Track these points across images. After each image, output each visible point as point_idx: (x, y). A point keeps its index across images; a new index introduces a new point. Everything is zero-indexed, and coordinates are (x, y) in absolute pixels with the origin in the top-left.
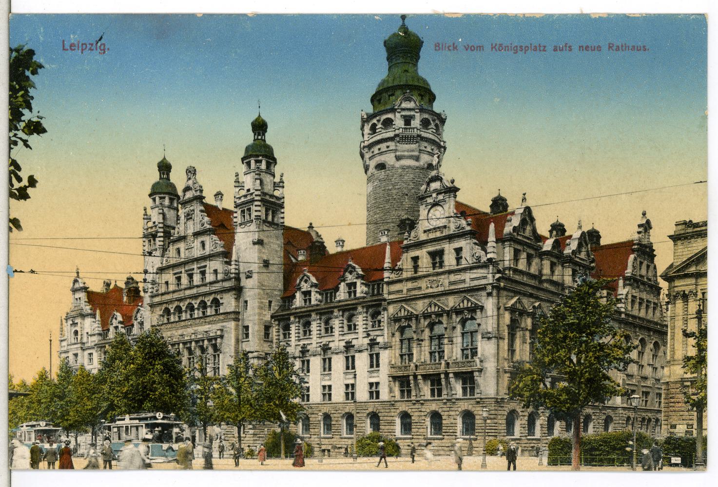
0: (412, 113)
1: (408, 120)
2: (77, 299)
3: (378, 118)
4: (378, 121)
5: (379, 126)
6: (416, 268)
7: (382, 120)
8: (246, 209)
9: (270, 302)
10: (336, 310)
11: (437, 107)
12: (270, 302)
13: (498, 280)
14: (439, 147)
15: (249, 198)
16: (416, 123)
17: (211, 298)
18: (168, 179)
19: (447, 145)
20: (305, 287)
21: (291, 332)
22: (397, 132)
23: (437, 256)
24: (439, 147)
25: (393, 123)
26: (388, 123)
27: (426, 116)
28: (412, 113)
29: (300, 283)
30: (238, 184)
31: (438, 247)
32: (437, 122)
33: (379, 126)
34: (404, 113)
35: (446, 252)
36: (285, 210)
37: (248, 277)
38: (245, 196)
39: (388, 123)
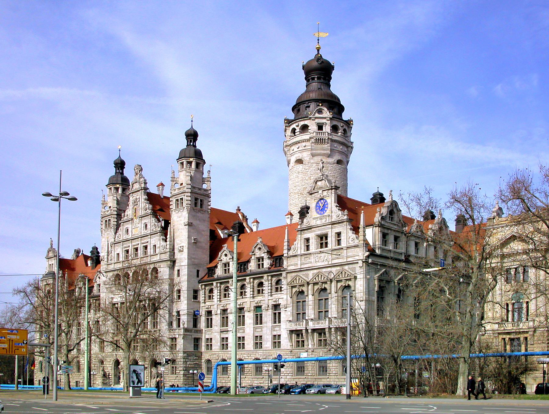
0: (324, 121)
1: (320, 127)
3: (297, 124)
4: (297, 126)
5: (298, 130)
6: (308, 247)
7: (300, 126)
8: (179, 198)
9: (198, 271)
10: (247, 278)
11: (345, 116)
12: (198, 271)
13: (368, 257)
14: (347, 147)
15: (182, 190)
16: (327, 129)
18: (122, 173)
19: (354, 145)
20: (225, 259)
21: (214, 294)
22: (312, 135)
23: (323, 239)
24: (347, 147)
25: (309, 128)
26: (305, 128)
27: (335, 123)
28: (324, 121)
29: (221, 256)
30: (174, 180)
31: (324, 232)
32: (345, 127)
33: (298, 130)
34: (317, 120)
35: (329, 236)
36: (212, 199)
38: (179, 189)
39: (305, 128)
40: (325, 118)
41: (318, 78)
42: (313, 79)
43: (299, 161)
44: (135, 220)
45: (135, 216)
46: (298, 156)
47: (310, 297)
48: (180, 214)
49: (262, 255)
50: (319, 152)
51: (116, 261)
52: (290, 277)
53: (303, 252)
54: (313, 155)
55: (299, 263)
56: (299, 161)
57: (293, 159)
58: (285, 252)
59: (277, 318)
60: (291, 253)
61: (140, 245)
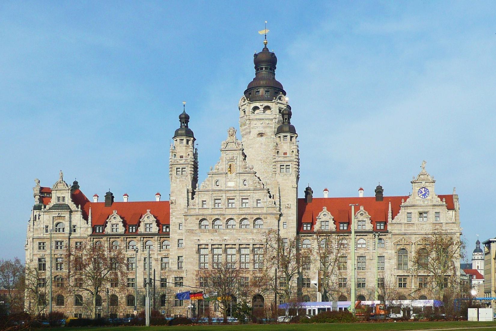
2: (59, 198)
3: (261, 104)
7: (263, 107)
33: (261, 109)
41: (266, 68)
42: (262, 69)
43: (261, 135)
44: (229, 174)
46: (262, 130)
48: (286, 177)
49: (364, 220)
52: (395, 239)
53: (406, 222)
55: (403, 228)
56: (261, 135)
57: (254, 132)
58: (390, 220)
61: (238, 197)
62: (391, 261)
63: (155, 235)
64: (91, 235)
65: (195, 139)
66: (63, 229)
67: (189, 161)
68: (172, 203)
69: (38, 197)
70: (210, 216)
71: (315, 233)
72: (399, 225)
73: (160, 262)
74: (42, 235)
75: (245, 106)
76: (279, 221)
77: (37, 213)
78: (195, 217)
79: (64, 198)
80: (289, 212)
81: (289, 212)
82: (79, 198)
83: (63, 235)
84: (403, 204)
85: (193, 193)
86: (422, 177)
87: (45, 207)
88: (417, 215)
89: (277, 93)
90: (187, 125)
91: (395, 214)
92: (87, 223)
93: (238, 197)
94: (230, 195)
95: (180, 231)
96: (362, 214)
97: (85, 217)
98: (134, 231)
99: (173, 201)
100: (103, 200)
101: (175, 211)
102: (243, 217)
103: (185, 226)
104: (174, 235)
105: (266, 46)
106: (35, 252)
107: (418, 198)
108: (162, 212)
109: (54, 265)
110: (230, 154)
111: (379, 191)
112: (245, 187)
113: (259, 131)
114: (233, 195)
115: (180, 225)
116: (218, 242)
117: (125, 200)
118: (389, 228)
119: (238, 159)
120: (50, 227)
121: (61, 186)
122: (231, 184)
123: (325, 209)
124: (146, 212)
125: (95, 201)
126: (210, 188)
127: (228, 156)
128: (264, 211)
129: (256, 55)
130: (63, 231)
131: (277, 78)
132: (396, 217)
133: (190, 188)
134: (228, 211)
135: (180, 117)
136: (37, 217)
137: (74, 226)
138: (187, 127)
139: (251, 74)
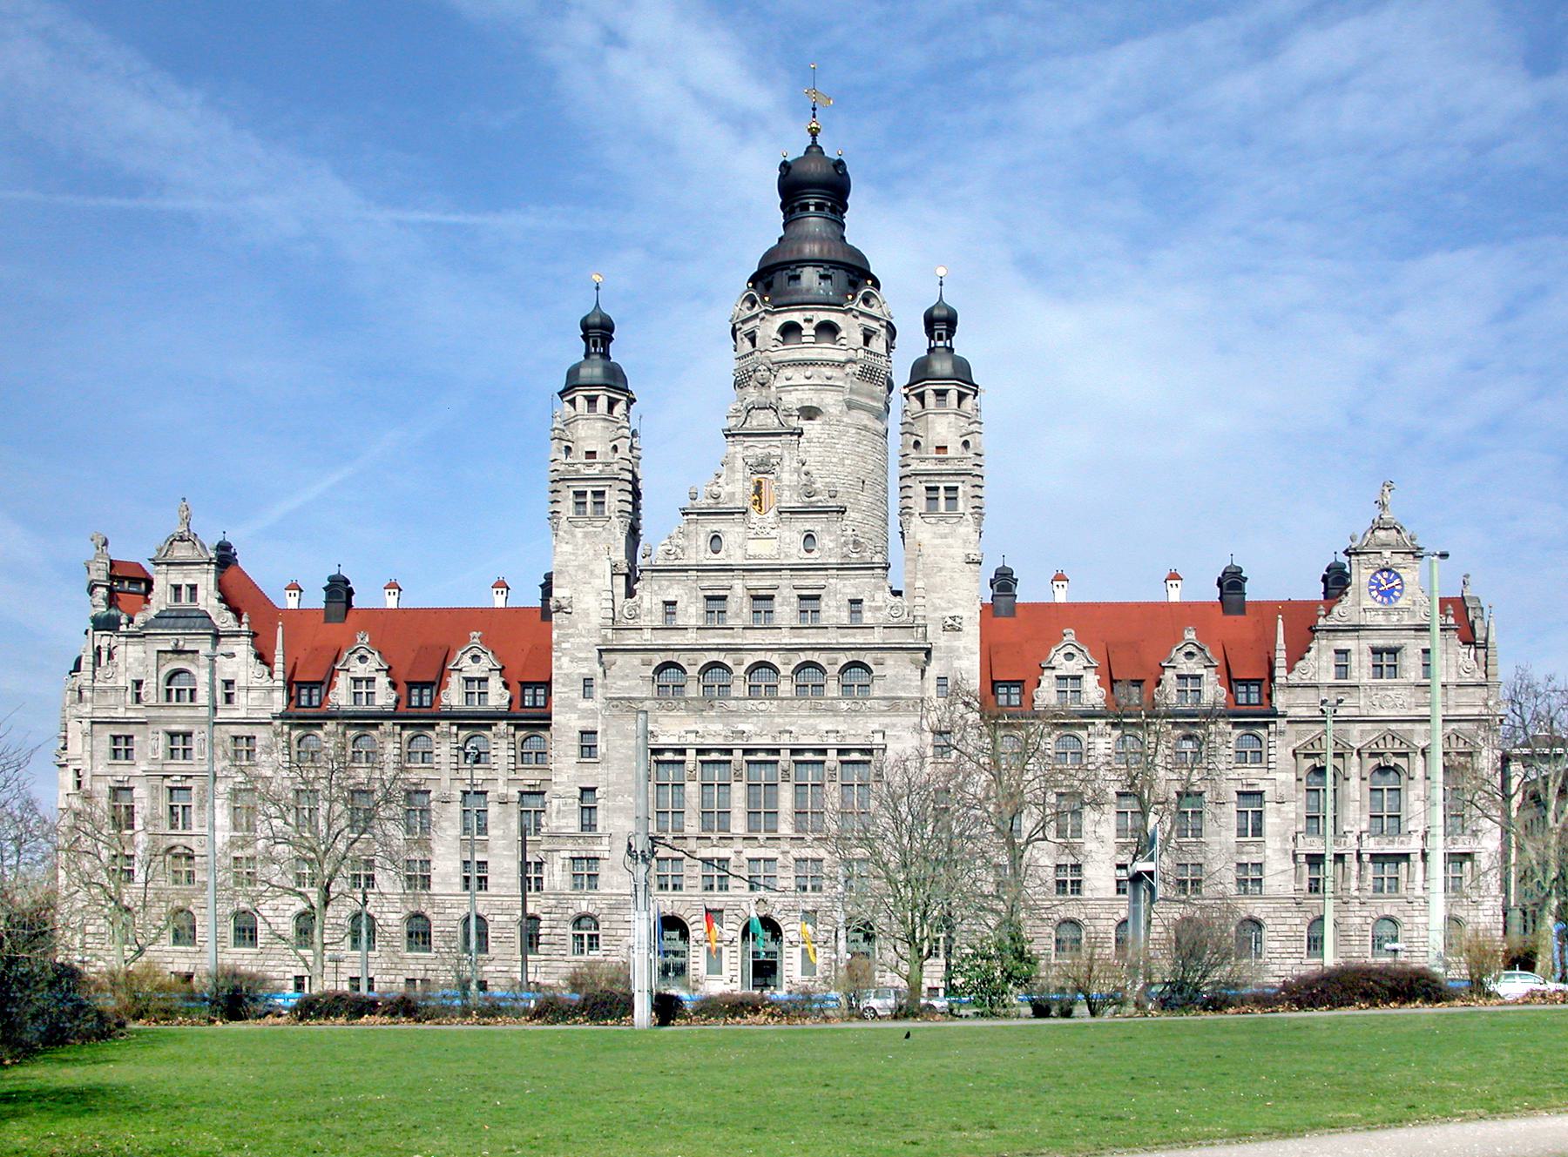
0: (874, 325)
2: (177, 588)
3: (808, 315)
4: (809, 321)
5: (808, 330)
6: (1343, 670)
8: (942, 486)
17: (844, 659)
23: (1386, 658)
25: (843, 334)
26: (828, 330)
28: (874, 325)
31: (1393, 643)
33: (808, 330)
34: (862, 320)
37: (953, 627)
40: (877, 319)
41: (819, 207)
42: (805, 207)
44: (754, 515)
45: (758, 502)
46: (811, 398)
47: (1355, 781)
48: (943, 528)
49: (1198, 672)
50: (864, 400)
51: (657, 624)
53: (1331, 679)
54: (850, 406)
58: (1280, 673)
59: (1255, 827)
60: (1294, 678)
61: (786, 592)
62: (1285, 807)
63: (497, 716)
64: (281, 717)
65: (631, 401)
66: (192, 691)
67: (616, 468)
68: (559, 609)
69: (102, 592)
70: (690, 655)
71: (1036, 716)
72: (1312, 692)
73: (514, 809)
74: (120, 713)
75: (757, 322)
76: (923, 671)
77: (104, 641)
78: (640, 656)
79: (193, 588)
80: (956, 643)
81: (956, 643)
82: (237, 593)
83: (191, 713)
84: (1321, 621)
85: (631, 578)
86: (1381, 534)
87: (131, 621)
88: (1368, 660)
89: (854, 286)
90: (606, 349)
91: (1297, 654)
92: (271, 675)
93: (786, 592)
94: (760, 582)
95: (588, 704)
96: (1190, 655)
97: (263, 658)
98: (426, 702)
99: (564, 603)
100: (316, 599)
101: (572, 636)
102: (804, 657)
103: (604, 686)
104: (567, 718)
105: (814, 141)
106: (100, 770)
107: (1368, 603)
108: (524, 637)
109: (163, 810)
110: (760, 448)
111: (1232, 582)
112: (815, 557)
113: (801, 400)
114: (768, 583)
115: (588, 683)
116: (719, 741)
117: (391, 602)
118: (1280, 700)
119: (786, 462)
120: (148, 689)
121: (182, 552)
122: (763, 550)
123: (1070, 636)
124: (467, 640)
125: (292, 603)
126: (691, 559)
127: (750, 452)
128: (876, 637)
129: (785, 166)
130: (192, 699)
131: (851, 238)
132: (1300, 664)
133: (620, 556)
134: (752, 638)
135: (586, 326)
136: (104, 654)
137: (229, 683)
138: (605, 355)
139: (765, 226)
